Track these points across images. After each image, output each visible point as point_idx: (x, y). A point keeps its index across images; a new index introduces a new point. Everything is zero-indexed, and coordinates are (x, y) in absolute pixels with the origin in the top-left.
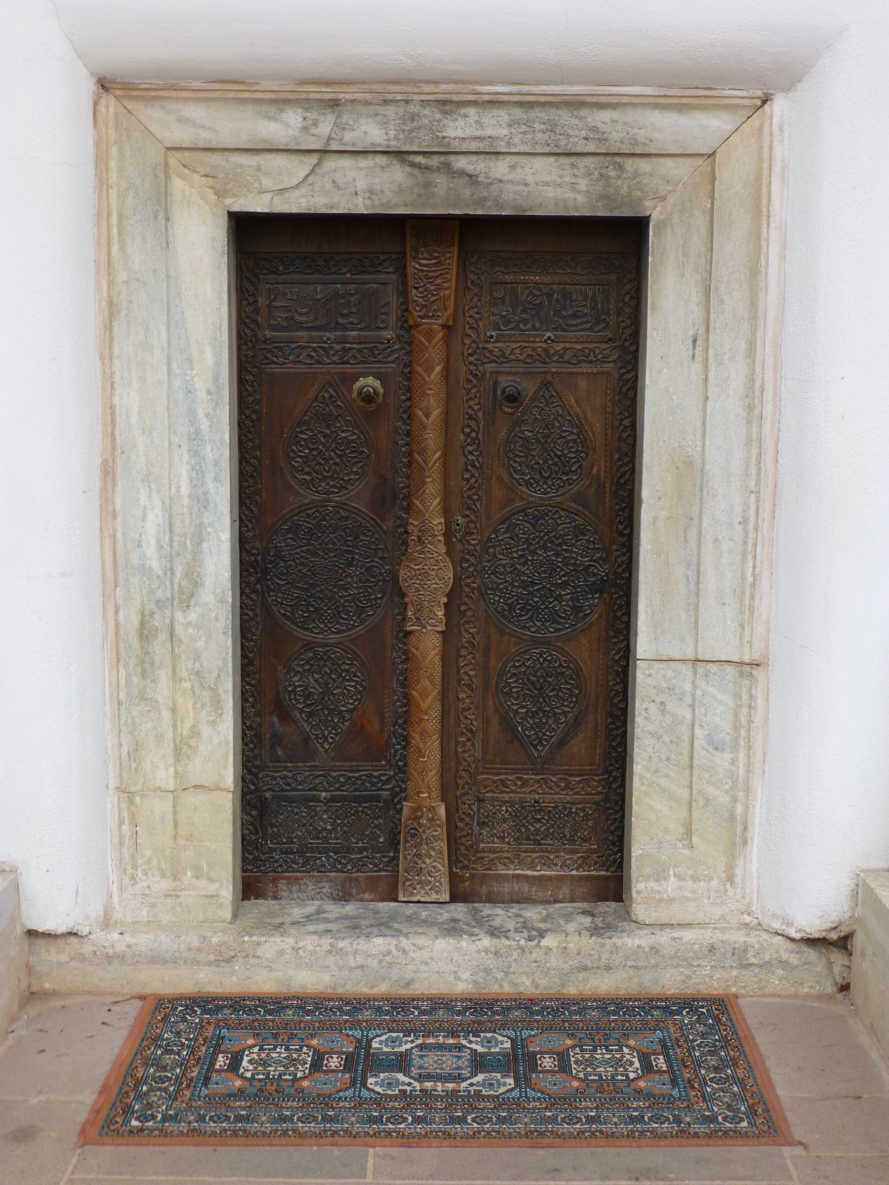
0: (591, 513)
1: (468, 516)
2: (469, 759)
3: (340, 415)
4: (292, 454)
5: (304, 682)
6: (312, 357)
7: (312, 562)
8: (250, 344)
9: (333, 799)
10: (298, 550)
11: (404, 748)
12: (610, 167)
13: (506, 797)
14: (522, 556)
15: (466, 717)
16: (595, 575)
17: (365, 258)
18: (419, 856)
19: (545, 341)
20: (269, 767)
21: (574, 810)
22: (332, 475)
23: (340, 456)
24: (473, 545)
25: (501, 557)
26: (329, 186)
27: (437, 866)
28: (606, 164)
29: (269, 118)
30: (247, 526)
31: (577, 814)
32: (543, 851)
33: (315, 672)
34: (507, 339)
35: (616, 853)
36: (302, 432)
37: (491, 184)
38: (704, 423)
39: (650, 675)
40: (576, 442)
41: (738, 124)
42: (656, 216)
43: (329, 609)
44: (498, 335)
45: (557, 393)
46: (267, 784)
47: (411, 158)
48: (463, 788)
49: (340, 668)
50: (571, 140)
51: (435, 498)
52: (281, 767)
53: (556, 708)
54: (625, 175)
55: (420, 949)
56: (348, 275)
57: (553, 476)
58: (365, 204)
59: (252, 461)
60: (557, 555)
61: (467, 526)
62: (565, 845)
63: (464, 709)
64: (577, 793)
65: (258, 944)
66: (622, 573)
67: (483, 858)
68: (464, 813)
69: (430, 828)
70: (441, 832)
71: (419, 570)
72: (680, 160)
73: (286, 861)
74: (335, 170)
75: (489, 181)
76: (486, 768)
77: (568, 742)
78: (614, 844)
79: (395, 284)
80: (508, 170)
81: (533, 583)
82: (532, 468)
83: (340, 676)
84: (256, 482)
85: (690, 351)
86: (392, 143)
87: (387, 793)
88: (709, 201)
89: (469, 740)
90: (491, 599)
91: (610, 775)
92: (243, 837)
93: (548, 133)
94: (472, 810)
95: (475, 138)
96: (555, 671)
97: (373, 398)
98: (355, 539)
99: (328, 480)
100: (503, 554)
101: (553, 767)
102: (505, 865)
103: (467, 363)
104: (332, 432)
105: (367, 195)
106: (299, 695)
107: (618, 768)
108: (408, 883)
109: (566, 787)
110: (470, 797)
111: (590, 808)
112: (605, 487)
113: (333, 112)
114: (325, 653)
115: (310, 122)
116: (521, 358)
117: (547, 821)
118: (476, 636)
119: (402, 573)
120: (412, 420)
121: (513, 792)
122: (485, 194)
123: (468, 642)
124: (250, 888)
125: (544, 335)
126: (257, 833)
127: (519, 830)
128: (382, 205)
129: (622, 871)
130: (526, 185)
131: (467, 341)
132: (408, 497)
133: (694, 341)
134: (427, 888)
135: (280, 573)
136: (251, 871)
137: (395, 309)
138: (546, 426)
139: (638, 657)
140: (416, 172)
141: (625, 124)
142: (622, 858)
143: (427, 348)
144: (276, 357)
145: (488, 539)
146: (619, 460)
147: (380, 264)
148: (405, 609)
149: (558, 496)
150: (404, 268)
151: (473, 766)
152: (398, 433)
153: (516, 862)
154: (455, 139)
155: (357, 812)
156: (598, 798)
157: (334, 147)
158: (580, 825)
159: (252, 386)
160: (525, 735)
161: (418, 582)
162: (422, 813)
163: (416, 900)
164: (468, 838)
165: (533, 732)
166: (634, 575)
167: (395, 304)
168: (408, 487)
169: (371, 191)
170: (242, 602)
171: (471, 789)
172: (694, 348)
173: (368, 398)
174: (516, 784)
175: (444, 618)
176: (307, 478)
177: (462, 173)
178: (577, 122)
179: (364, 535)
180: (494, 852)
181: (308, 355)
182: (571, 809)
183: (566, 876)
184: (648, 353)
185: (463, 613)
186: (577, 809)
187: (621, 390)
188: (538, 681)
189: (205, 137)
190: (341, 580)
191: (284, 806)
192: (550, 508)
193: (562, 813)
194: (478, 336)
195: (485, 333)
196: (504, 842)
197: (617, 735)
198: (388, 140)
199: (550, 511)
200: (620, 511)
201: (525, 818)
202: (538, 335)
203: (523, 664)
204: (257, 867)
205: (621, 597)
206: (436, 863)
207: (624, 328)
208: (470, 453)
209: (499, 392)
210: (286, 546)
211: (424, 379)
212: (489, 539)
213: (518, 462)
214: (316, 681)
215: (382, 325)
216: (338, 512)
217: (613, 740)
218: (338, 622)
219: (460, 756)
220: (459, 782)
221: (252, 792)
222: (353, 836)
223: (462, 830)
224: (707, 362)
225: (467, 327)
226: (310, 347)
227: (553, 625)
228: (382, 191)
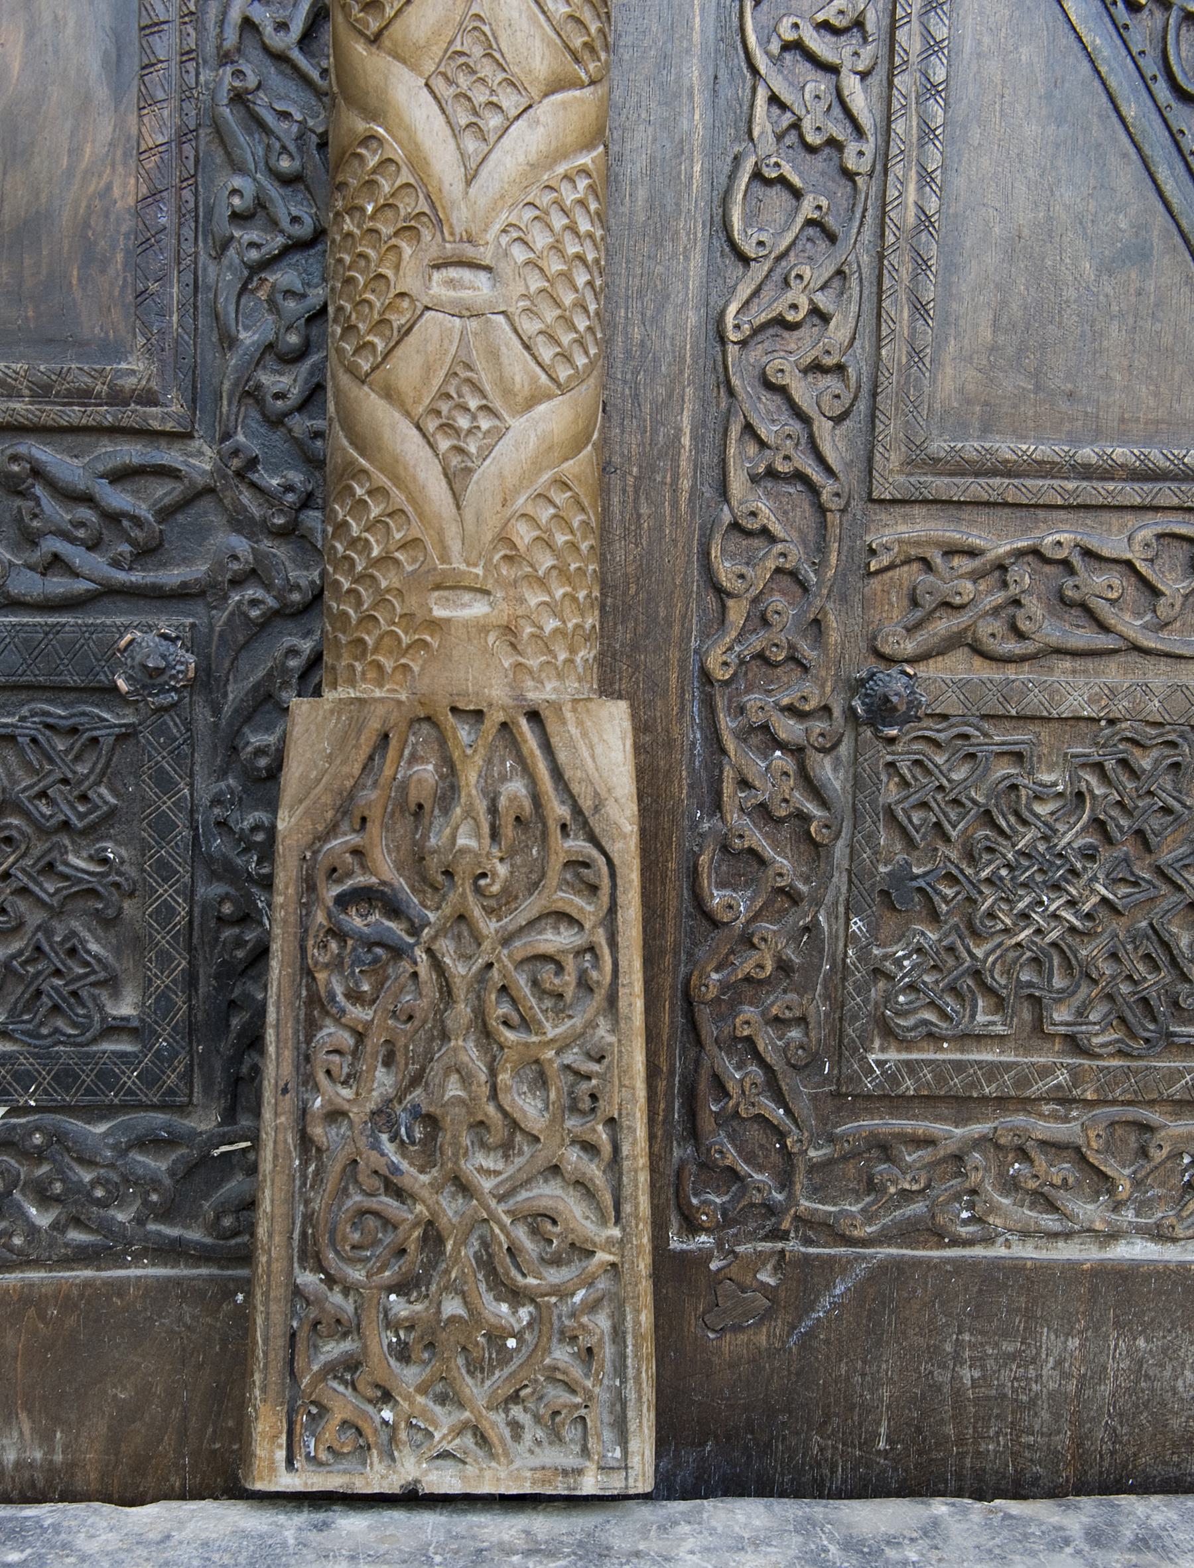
67: (884, 1148)
68: (763, 812)
69: (506, 900)
76: (935, 465)
108: (333, 1350)
162: (450, 768)
163: (392, 1484)
180: (963, 1105)
206: (548, 1193)
219: (742, 369)
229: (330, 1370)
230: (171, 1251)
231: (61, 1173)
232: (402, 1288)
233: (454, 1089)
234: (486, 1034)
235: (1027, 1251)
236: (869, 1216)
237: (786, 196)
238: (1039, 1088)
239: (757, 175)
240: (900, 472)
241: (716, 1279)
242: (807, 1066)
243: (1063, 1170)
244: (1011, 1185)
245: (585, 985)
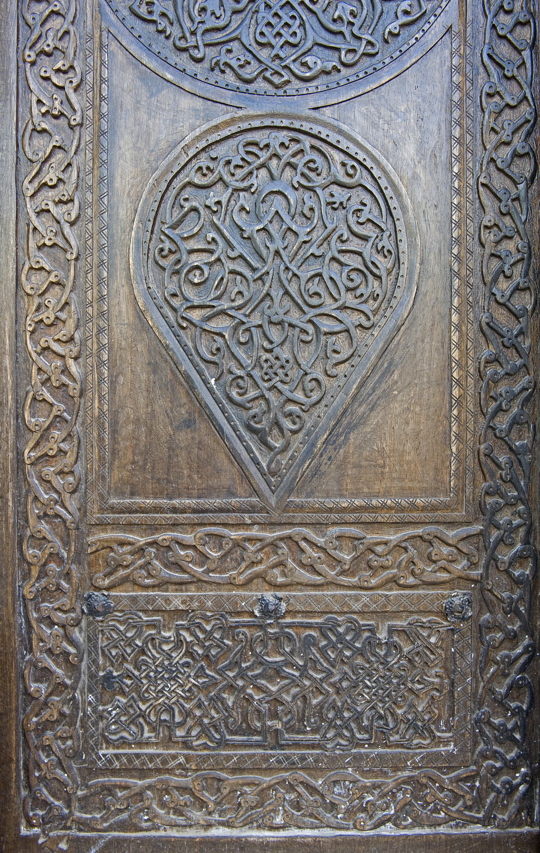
2: (58, 482)
13: (177, 599)
21: (382, 635)
31: (396, 647)
32: (292, 766)
48: (43, 573)
64: (394, 581)
67: (109, 790)
68: (50, 652)
76: (112, 509)
77: (363, 420)
94: (72, 642)
101: (315, 501)
102: (178, 812)
111: (431, 627)
117: (303, 670)
118: (73, 98)
121: (198, 582)
151: (72, 503)
156: (458, 597)
160: (231, 400)
164: (62, 729)
165: (252, 393)
171: (68, 576)
174: (205, 557)
182: (372, 630)
183: (366, 841)
186: (391, 631)
193: (349, 646)
196: (169, 741)
217: (499, 409)
220: (30, 552)
235: (174, 833)
236: (104, 819)
237: (47, 405)
238: (172, 764)
239: (34, 399)
240: (99, 513)
241: (41, 847)
242: (76, 755)
244: (163, 805)
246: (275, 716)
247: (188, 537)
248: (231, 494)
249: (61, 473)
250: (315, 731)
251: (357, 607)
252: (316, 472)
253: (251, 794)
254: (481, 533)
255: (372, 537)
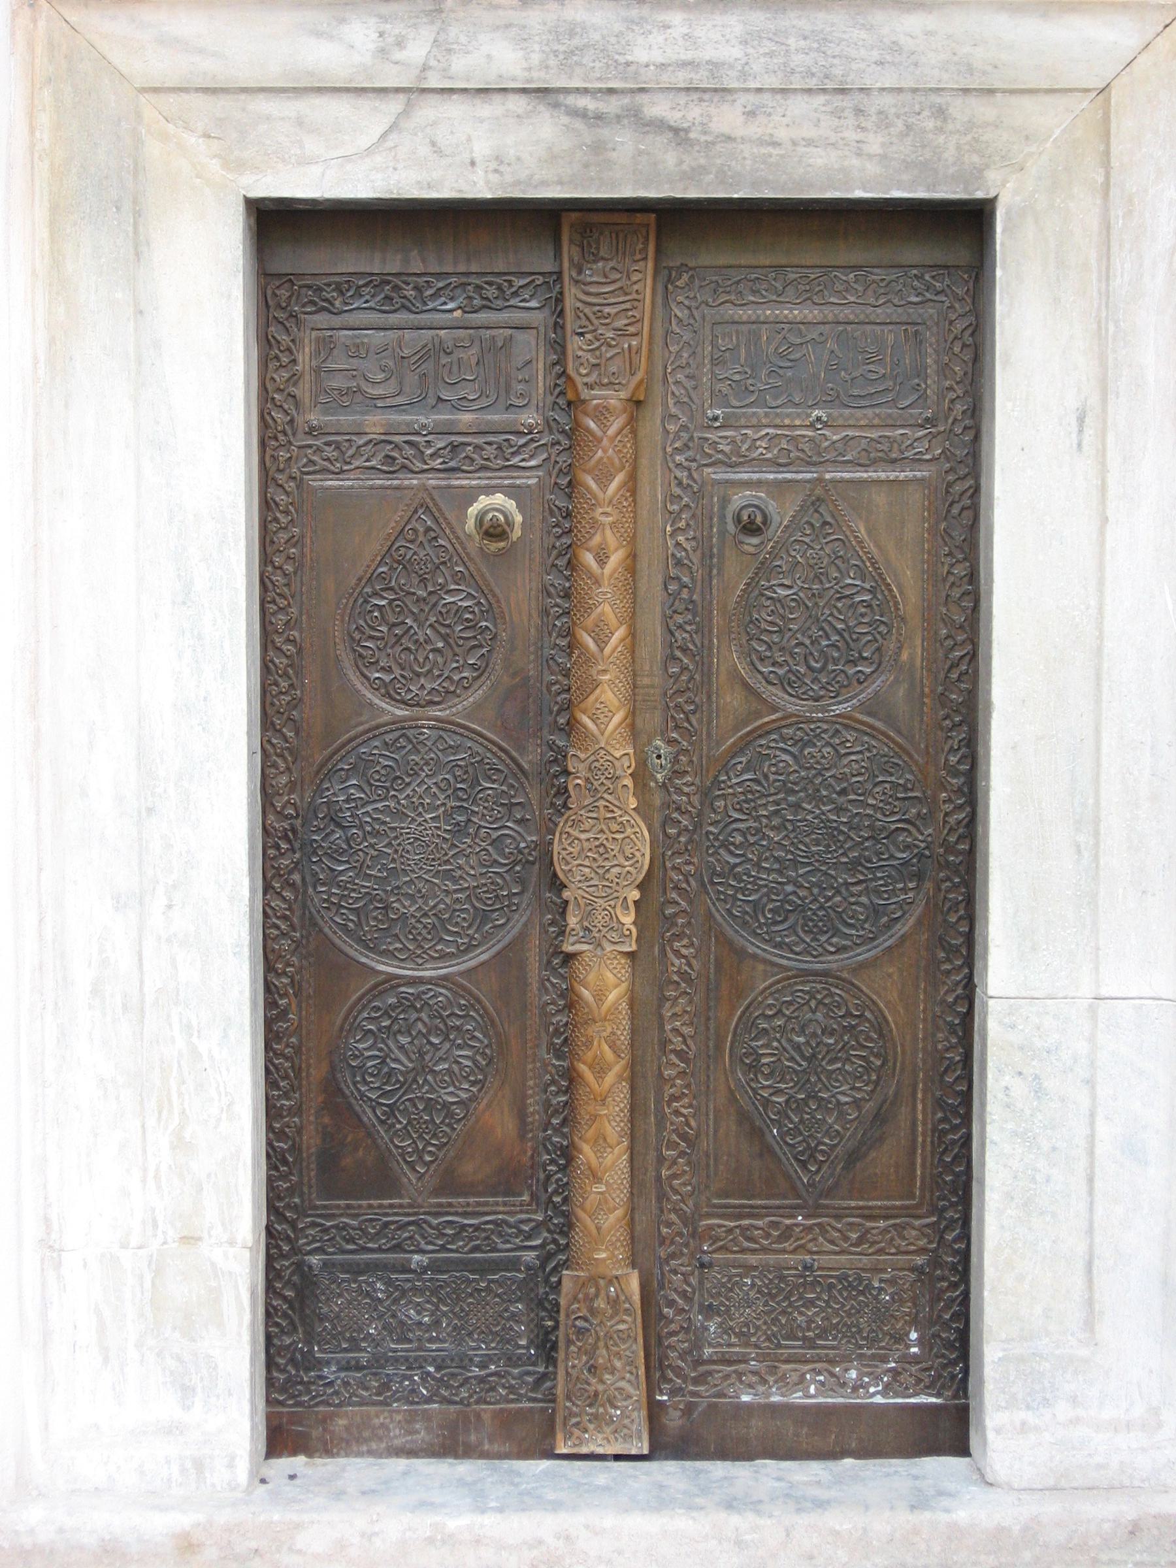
0: (899, 732)
1: (676, 740)
3: (444, 563)
4: (357, 636)
5: (380, 1050)
6: (394, 459)
7: (395, 828)
8: (281, 437)
9: (436, 1267)
10: (369, 808)
11: (563, 1169)
12: (926, 113)
14: (776, 812)
15: (677, 1113)
16: (908, 847)
17: (490, 284)
18: (592, 1369)
19: (812, 425)
20: (316, 1208)
22: (430, 671)
23: (445, 637)
24: (687, 794)
25: (736, 815)
26: (424, 150)
27: (625, 1384)
28: (917, 108)
29: (319, 34)
30: (274, 765)
32: (820, 1360)
33: (399, 1031)
34: (743, 422)
35: (954, 1363)
36: (376, 594)
37: (713, 143)
38: (1101, 567)
39: (1013, 1027)
40: (869, 606)
41: (1149, 37)
42: (1010, 196)
43: (425, 915)
44: (727, 417)
45: (833, 516)
46: (314, 1241)
47: (571, 100)
49: (446, 1024)
50: (854, 66)
51: (618, 710)
52: (338, 1207)
53: (843, 1093)
54: (950, 127)
55: (596, 1534)
56: (458, 314)
57: (831, 667)
58: (487, 182)
59: (284, 647)
60: (839, 810)
61: (676, 760)
62: (861, 1347)
63: (674, 1098)
64: (880, 1251)
65: (298, 1526)
66: (957, 843)
67: (710, 1373)
68: (675, 1290)
69: (612, 1317)
70: (630, 1324)
71: (588, 840)
72: (1048, 99)
73: (346, 1384)
74: (434, 124)
75: (709, 138)
76: (715, 1206)
77: (865, 1155)
78: (949, 1345)
79: (542, 329)
80: (742, 119)
81: (795, 863)
82: (792, 655)
83: (447, 1038)
84: (292, 686)
85: (1074, 436)
86: (535, 74)
87: (533, 1254)
88: (1101, 171)
89: (682, 1154)
90: (719, 892)
91: (941, 1217)
92: (269, 1338)
93: (813, 55)
94: (689, 1285)
95: (685, 64)
96: (839, 1024)
97: (504, 532)
98: (472, 787)
99: (422, 681)
100: (741, 810)
103: (671, 465)
104: (431, 593)
105: (493, 165)
106: (372, 1075)
107: (957, 1204)
109: (859, 1242)
110: (684, 1260)
112: (922, 687)
113: (432, 22)
114: (418, 997)
115: (391, 40)
116: (769, 456)
118: (694, 962)
119: (556, 847)
120: (573, 569)
121: (765, 1250)
122: (702, 161)
123: (679, 973)
124: (283, 1436)
125: (809, 416)
126: (295, 1329)
127: (775, 1321)
128: (517, 183)
129: (966, 1396)
130: (776, 144)
131: (672, 428)
132: (568, 707)
133: (1081, 420)
134: (608, 1430)
135: (336, 851)
136: (281, 1403)
137: (541, 373)
138: (816, 576)
139: (990, 992)
140: (579, 124)
141: (949, 37)
142: (966, 1371)
143: (600, 441)
144: (328, 459)
145: (712, 783)
146: (948, 637)
147: (515, 294)
148: (563, 913)
149: (840, 703)
150: (560, 299)
151: (691, 1203)
152: (549, 595)
153: (771, 1379)
154: (647, 66)
155: (479, 1291)
156: (919, 1260)
157: (434, 82)
158: (888, 1309)
159: (287, 513)
161: (587, 863)
164: (681, 1336)
166: (980, 846)
167: (541, 365)
168: (569, 689)
169: (499, 159)
170: (266, 905)
172: (1081, 431)
173: (494, 531)
175: (634, 930)
176: (387, 678)
177: (660, 125)
178: (863, 34)
179: (489, 779)
180: (729, 1363)
181: (387, 456)
184: (997, 441)
185: (670, 920)
187: (948, 511)
188: (808, 1043)
189: (209, 68)
190: (447, 862)
191: (343, 1281)
192: (825, 727)
193: (854, 1288)
194: (691, 418)
195: (704, 413)
196: (747, 1344)
197: (954, 1142)
198: (530, 69)
199: (825, 731)
200: (951, 730)
201: (786, 1298)
202: (799, 415)
203: (780, 1012)
204: (293, 1397)
205: (956, 886)
206: (622, 1384)
207: (952, 401)
208: (680, 627)
209: (729, 520)
210: (347, 801)
211: (595, 498)
212: (716, 782)
213: (765, 642)
214: (401, 1047)
215: (518, 402)
216: (441, 737)
217: (945, 1150)
218: (442, 939)
221: (283, 1256)
222: (470, 1334)
223: (672, 1321)
224: (1104, 455)
225: (671, 402)
226: (390, 442)
227: (834, 940)
228: (519, 159)
229: (574, 1425)
230: (535, 1400)
231: (508, 1381)
232: (590, 1405)
233: (601, 1361)
234: (607, 1348)
236: (707, 1391)
242: (691, 1352)
243: (754, 1379)
245: (629, 1336)
246: (809, 1330)
247: (760, 1223)
248: (785, 1198)
249: (685, 1184)
250: (834, 1339)
251: (861, 1265)
252: (837, 1185)
253: (795, 1377)
254: (934, 1223)
255: (869, 1224)
